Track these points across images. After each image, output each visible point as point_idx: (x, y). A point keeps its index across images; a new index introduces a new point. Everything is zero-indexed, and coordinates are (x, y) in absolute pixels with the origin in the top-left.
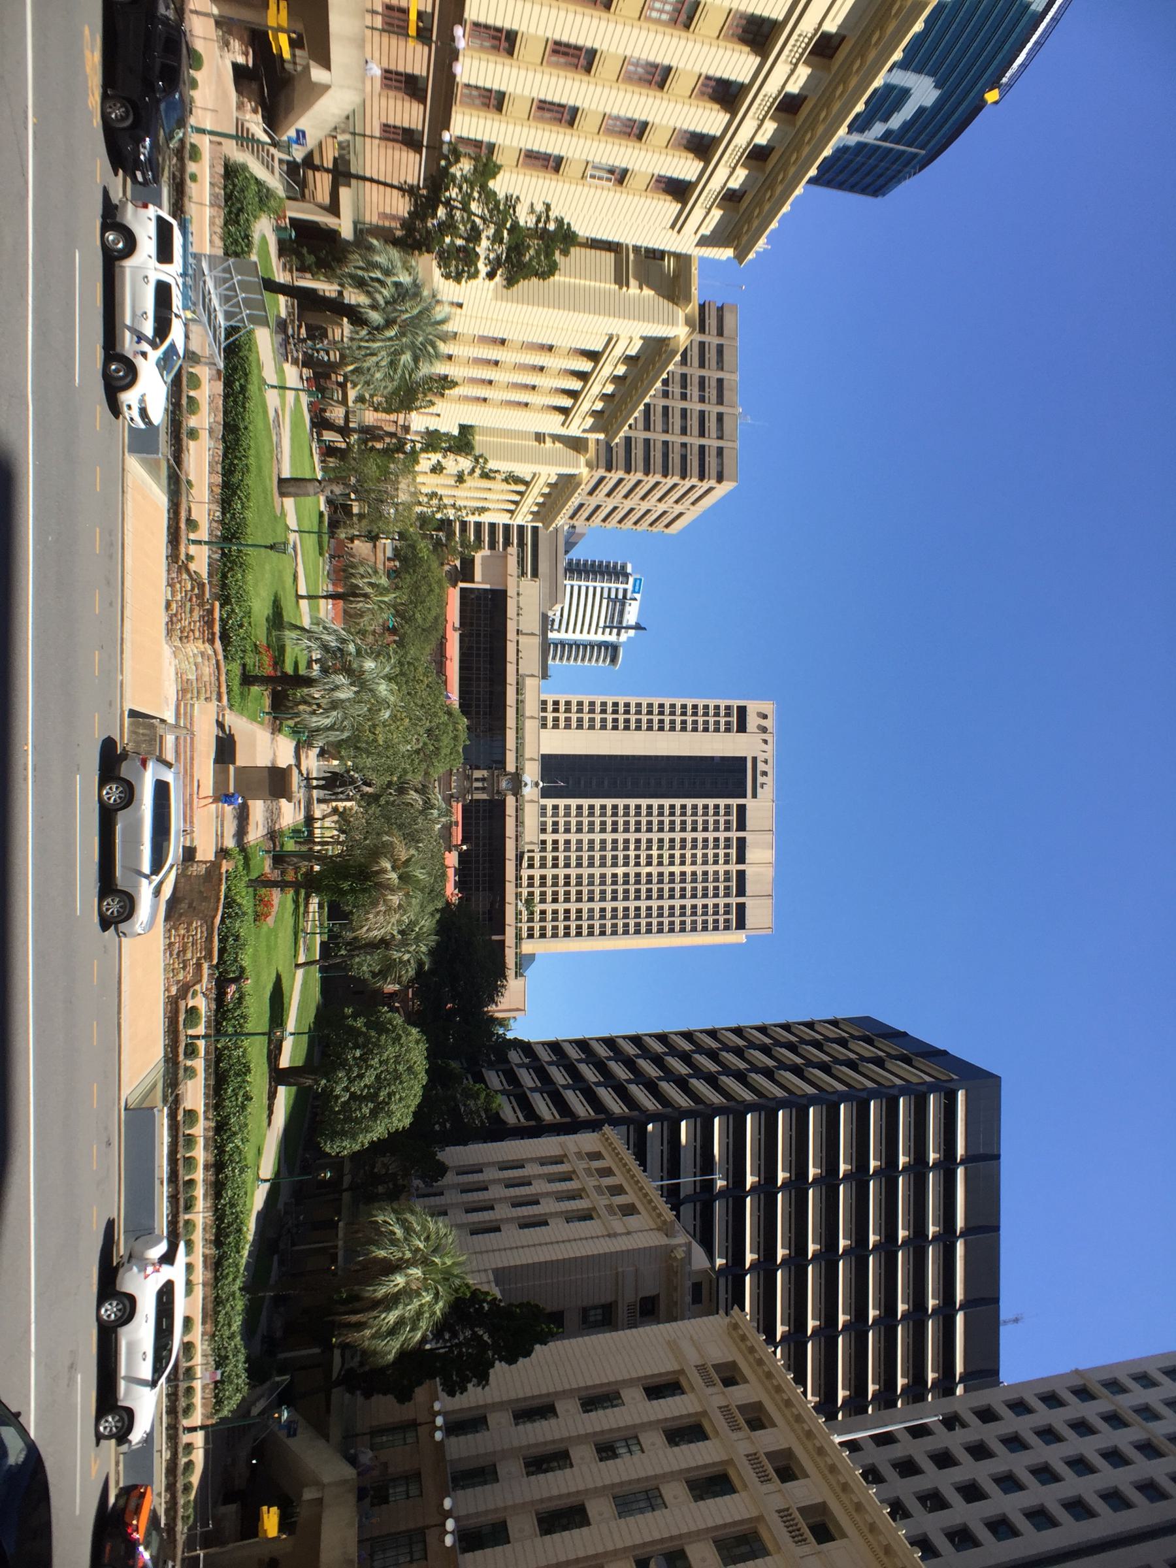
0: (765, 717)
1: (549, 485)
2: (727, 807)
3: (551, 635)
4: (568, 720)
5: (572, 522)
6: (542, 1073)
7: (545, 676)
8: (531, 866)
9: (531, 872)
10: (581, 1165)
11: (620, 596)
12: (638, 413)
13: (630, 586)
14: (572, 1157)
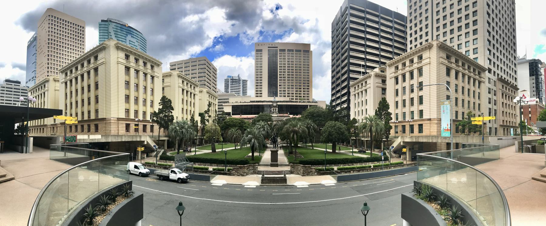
7: (250, 96)
12: (193, 79)
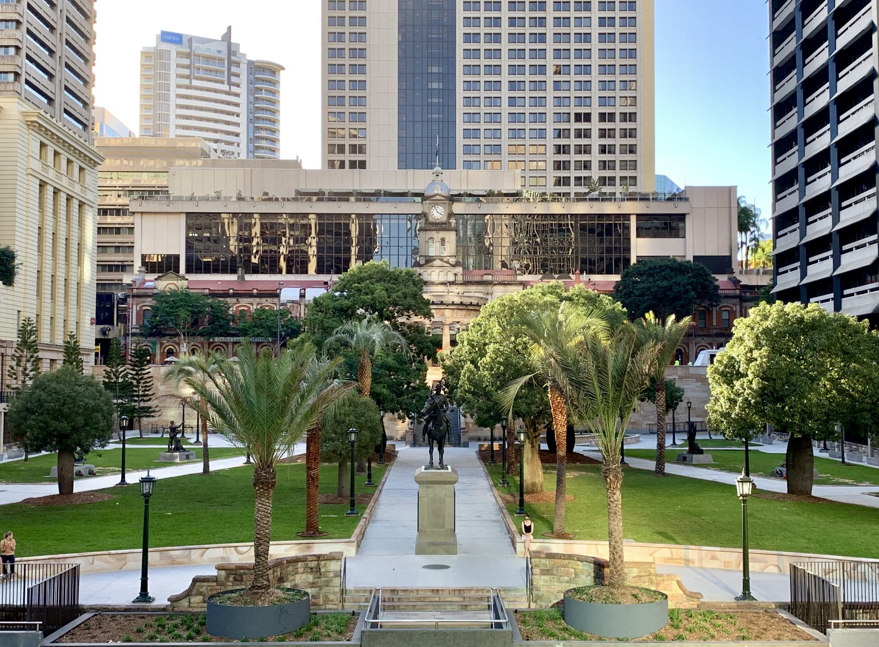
3: (243, 156)
11: (187, 62)
13: (173, 48)
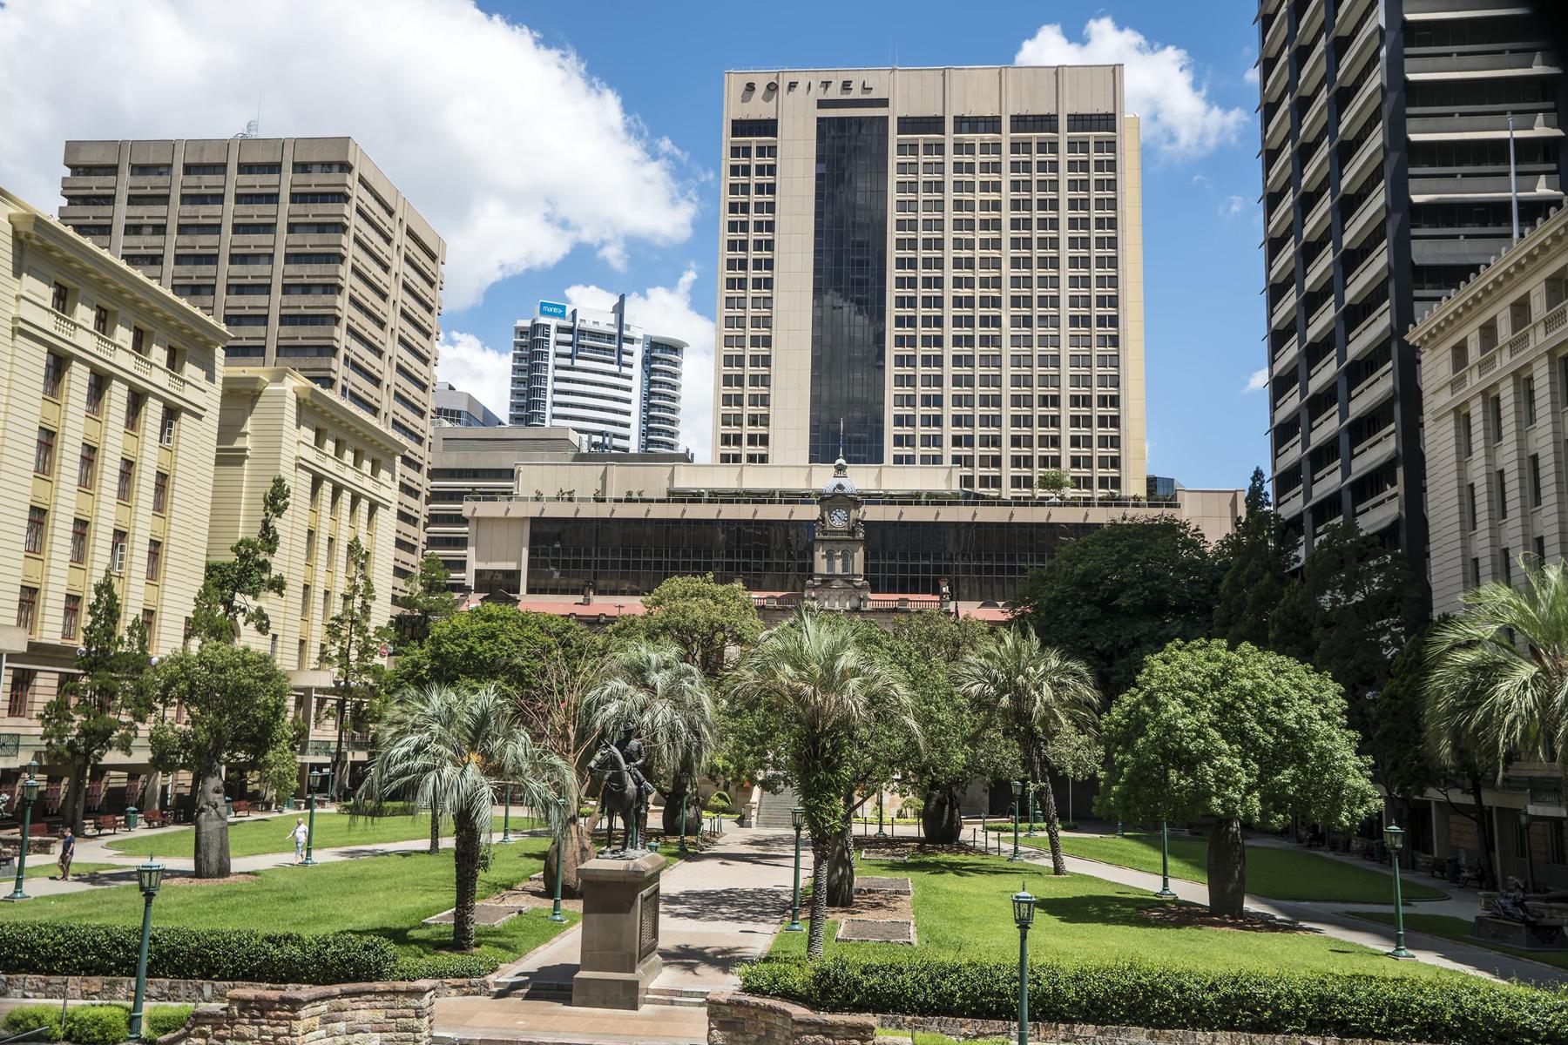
0: (750, 87)
1: (319, 442)
2: (901, 149)
4: (753, 421)
5: (429, 414)
6: (1322, 456)
8: (997, 482)
9: (1006, 482)
10: (1475, 381)
14: (1461, 395)
